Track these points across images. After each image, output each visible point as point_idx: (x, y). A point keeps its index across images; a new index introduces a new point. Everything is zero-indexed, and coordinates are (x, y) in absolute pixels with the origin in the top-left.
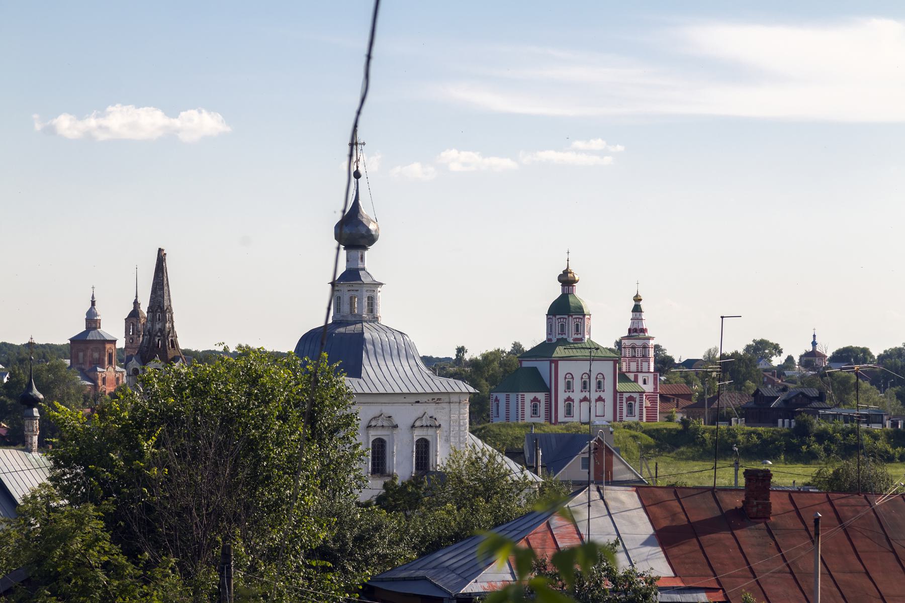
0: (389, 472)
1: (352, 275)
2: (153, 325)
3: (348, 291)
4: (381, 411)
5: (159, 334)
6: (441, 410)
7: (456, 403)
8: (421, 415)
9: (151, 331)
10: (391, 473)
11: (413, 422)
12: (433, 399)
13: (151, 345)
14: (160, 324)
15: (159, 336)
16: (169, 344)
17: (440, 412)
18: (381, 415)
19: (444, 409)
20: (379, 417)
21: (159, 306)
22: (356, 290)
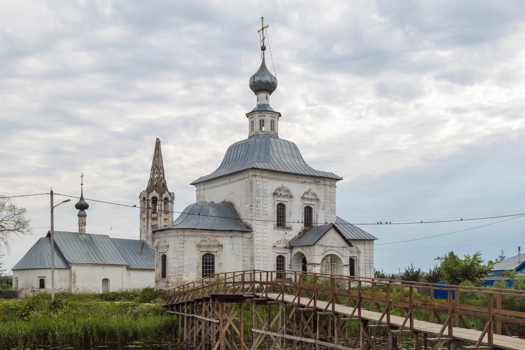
0: (288, 226)
2: (153, 176)
3: (259, 116)
4: (283, 185)
5: (156, 180)
6: (320, 189)
7: (329, 185)
8: (308, 191)
9: (152, 179)
10: (289, 227)
11: (303, 194)
12: (315, 181)
13: (152, 185)
14: (157, 175)
15: (156, 181)
16: (161, 185)
17: (319, 190)
18: (283, 187)
19: (321, 188)
20: (281, 188)
21: (157, 166)
22: (264, 116)
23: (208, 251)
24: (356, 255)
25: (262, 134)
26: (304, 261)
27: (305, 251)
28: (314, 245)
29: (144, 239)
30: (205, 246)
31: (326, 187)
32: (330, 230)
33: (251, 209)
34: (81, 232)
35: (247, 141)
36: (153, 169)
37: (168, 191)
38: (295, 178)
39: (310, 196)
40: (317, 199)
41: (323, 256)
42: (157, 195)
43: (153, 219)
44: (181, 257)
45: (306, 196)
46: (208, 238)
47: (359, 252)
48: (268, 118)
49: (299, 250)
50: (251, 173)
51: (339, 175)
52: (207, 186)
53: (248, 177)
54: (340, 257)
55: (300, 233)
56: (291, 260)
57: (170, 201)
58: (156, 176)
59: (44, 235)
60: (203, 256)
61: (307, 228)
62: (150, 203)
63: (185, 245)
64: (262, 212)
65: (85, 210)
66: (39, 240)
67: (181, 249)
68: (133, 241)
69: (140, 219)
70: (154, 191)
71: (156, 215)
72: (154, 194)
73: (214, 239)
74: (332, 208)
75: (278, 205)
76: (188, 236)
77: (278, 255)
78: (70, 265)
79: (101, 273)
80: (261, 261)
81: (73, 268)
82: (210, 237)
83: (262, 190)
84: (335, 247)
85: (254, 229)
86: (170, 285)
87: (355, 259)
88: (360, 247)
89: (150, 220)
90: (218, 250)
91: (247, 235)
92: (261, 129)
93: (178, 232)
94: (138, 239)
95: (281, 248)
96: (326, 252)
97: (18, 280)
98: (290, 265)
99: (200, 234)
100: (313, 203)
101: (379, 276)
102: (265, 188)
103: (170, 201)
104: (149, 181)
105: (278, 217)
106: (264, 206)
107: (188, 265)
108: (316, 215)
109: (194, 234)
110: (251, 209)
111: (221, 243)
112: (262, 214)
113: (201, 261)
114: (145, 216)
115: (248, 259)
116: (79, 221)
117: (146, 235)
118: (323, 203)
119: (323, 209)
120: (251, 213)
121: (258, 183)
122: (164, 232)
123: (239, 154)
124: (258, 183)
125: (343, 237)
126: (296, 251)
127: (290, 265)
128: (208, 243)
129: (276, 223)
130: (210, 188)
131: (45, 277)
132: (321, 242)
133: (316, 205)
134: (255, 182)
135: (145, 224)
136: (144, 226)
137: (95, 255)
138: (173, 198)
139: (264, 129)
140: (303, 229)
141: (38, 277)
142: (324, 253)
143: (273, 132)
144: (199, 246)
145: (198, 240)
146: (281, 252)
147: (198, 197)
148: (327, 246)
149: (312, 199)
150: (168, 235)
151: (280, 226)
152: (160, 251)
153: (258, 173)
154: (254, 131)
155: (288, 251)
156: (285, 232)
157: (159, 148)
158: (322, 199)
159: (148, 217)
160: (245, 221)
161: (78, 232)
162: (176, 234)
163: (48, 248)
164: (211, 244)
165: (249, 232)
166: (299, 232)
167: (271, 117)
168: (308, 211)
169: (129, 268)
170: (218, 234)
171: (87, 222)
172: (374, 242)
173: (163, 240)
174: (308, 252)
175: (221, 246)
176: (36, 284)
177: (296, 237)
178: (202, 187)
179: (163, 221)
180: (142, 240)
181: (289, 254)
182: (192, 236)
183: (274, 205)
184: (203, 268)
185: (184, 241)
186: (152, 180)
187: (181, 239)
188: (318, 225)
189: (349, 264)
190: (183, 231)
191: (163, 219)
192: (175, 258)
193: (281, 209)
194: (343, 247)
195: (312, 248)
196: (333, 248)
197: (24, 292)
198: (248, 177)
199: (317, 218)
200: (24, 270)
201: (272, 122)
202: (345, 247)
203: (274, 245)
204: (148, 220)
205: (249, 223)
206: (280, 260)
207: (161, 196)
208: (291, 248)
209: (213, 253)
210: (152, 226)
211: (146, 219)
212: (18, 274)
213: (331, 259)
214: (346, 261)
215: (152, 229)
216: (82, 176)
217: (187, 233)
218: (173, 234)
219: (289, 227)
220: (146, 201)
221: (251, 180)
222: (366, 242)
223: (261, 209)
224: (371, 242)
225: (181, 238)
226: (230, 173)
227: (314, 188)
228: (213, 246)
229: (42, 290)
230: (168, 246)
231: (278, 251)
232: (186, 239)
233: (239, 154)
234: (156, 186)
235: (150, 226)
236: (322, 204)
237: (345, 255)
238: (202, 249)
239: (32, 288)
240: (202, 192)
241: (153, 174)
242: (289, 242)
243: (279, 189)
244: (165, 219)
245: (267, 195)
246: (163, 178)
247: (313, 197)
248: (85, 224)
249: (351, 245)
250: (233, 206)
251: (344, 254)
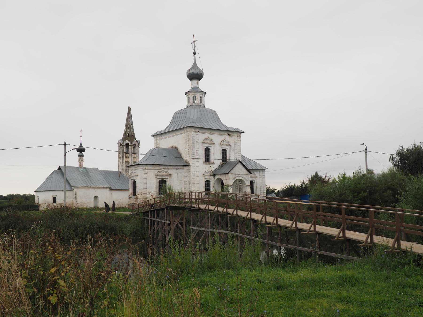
1: (195, 90)
2: (126, 130)
4: (208, 136)
8: (223, 140)
19: (232, 138)
23: (162, 178)
24: (254, 179)
25: (195, 105)
26: (222, 183)
27: (223, 177)
28: (228, 173)
29: (120, 170)
30: (160, 175)
31: (235, 137)
32: (238, 164)
34: (81, 166)
35: (185, 109)
36: (126, 126)
37: (136, 140)
38: (215, 132)
39: (225, 143)
40: (229, 145)
41: (234, 180)
42: (129, 143)
43: (126, 157)
44: (145, 182)
45: (222, 143)
46: (162, 170)
47: (256, 177)
48: (198, 95)
49: (219, 177)
50: (189, 129)
51: (242, 129)
52: (161, 137)
53: (187, 132)
54: (244, 180)
55: (219, 166)
56: (214, 183)
57: (137, 146)
58: (128, 130)
59: (57, 169)
60: (159, 181)
61: (224, 163)
62: (125, 147)
63: (148, 174)
64: (195, 153)
65: (83, 153)
66: (53, 172)
67: (145, 177)
68: (113, 172)
69: (118, 158)
70: (127, 140)
71: (128, 155)
72: (127, 141)
73: (166, 170)
74: (239, 150)
75: (205, 149)
76: (150, 169)
77: (206, 180)
78: (73, 188)
79: (93, 193)
80: (196, 184)
81: (75, 190)
82: (164, 170)
83: (195, 140)
84: (241, 174)
87: (254, 181)
88: (257, 174)
89: (124, 158)
90: (168, 177)
92: (194, 102)
93: (143, 167)
94: (117, 170)
95: (207, 176)
96: (235, 178)
97: (39, 198)
98: (213, 186)
99: (157, 168)
100: (227, 147)
101: (269, 191)
102: (197, 138)
103: (137, 146)
104: (124, 133)
105: (205, 156)
106: (197, 150)
107: (150, 187)
108: (229, 154)
109: (154, 167)
110: (189, 152)
111: (170, 173)
112: (195, 155)
114: (121, 155)
115: (187, 183)
116: (79, 159)
117: (122, 168)
118: (233, 147)
119: (233, 150)
120: (189, 154)
121: (193, 135)
122: (135, 166)
123: (180, 117)
124: (193, 135)
125: (246, 168)
126: (217, 177)
127: (213, 186)
128: (162, 173)
129: (204, 160)
130: (163, 138)
131: (57, 196)
132: (232, 171)
133: (229, 148)
134: (191, 135)
135: (121, 161)
136: (121, 162)
137: (89, 181)
138: (139, 144)
139: (196, 102)
140: (221, 163)
141: (52, 196)
142: (234, 178)
143: (201, 104)
144: (157, 175)
145: (156, 171)
146: (208, 178)
147: (156, 144)
148: (236, 174)
149: (226, 145)
150: (137, 168)
151: (207, 162)
152: (132, 178)
153: (193, 130)
154: (190, 103)
155: (212, 177)
156: (211, 165)
157: (130, 113)
158: (232, 144)
159: (123, 156)
160: (185, 159)
161: (78, 166)
162: (142, 168)
163: (59, 178)
164: (164, 174)
165: (187, 166)
166: (219, 165)
167: (200, 94)
168: (224, 152)
169: (111, 189)
170: (168, 168)
171: (84, 160)
172: (265, 170)
173: (134, 171)
174: (225, 178)
175: (170, 175)
176: (51, 200)
177: (217, 168)
178: (158, 138)
179: (133, 159)
180: (119, 171)
181: (213, 179)
182: (152, 169)
183: (203, 149)
185: (147, 172)
186: (126, 133)
187: (145, 171)
188: (231, 161)
189: (250, 185)
190: (146, 166)
191: (132, 157)
192: (141, 183)
193: (207, 151)
194: (246, 174)
195: (227, 175)
196: (239, 175)
197: (43, 206)
198: (187, 132)
199: (230, 156)
200: (43, 191)
201: (201, 97)
202: (247, 174)
203: (203, 174)
205: (188, 160)
206: (207, 183)
207: (131, 143)
208: (214, 175)
209: (165, 180)
211: (122, 158)
212: (39, 194)
213: (239, 182)
214: (248, 183)
215: (126, 164)
216: (81, 131)
217: (149, 167)
218: (140, 168)
219: (213, 162)
221: (189, 134)
222: (260, 171)
223: (195, 151)
224: (263, 171)
225: (145, 170)
226: (175, 129)
227: (227, 138)
228: (165, 175)
229: (55, 204)
230: (137, 175)
231: (206, 178)
233: (180, 117)
234: (128, 136)
235: (124, 162)
236: (233, 148)
237: (248, 180)
238: (158, 177)
239: (48, 203)
240: (158, 141)
241: (126, 129)
242: (213, 172)
243: (206, 139)
244: (134, 158)
245: (198, 143)
246: (133, 131)
247: (227, 144)
248: (82, 161)
249: (251, 173)
250: (178, 149)
251: (247, 178)
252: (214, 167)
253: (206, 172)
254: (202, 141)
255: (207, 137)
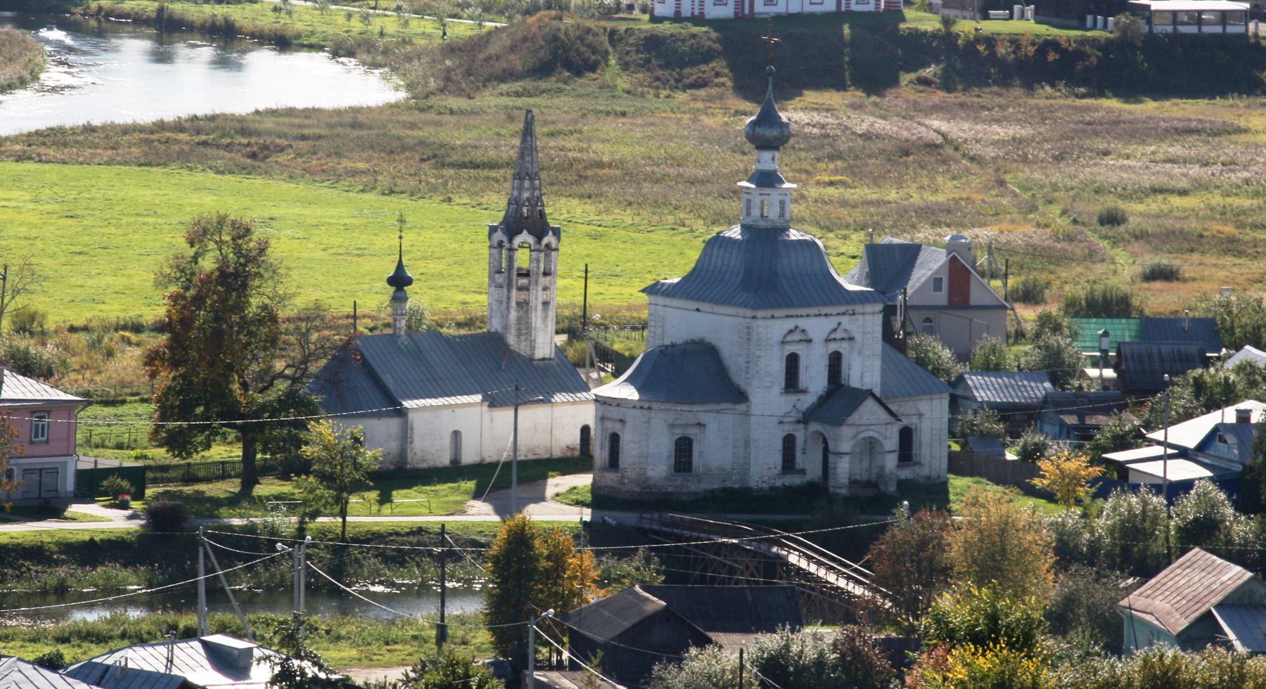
33: (748, 367)
39: (839, 335)
43: (520, 289)
47: (920, 415)
54: (881, 439)
77: (785, 434)
85: (751, 398)
86: (626, 481)
87: (913, 427)
91: (742, 407)
96: (858, 434)
111: (702, 422)
113: (674, 447)
114: (500, 279)
124: (760, 330)
132: (851, 420)
144: (672, 426)
158: (858, 337)
168: (835, 361)
178: (660, 300)
184: (676, 457)
193: (792, 363)
204: (509, 291)
206: (789, 441)
210: (518, 304)
215: (518, 312)
220: (504, 252)
232: (652, 414)
235: (513, 304)
238: (675, 431)
252: (808, 401)
253: (786, 415)
254: (780, 338)
255: (792, 327)
